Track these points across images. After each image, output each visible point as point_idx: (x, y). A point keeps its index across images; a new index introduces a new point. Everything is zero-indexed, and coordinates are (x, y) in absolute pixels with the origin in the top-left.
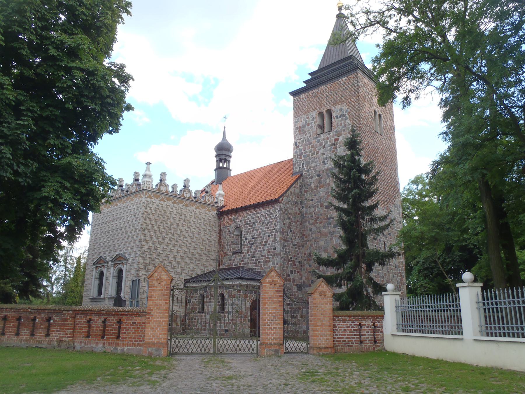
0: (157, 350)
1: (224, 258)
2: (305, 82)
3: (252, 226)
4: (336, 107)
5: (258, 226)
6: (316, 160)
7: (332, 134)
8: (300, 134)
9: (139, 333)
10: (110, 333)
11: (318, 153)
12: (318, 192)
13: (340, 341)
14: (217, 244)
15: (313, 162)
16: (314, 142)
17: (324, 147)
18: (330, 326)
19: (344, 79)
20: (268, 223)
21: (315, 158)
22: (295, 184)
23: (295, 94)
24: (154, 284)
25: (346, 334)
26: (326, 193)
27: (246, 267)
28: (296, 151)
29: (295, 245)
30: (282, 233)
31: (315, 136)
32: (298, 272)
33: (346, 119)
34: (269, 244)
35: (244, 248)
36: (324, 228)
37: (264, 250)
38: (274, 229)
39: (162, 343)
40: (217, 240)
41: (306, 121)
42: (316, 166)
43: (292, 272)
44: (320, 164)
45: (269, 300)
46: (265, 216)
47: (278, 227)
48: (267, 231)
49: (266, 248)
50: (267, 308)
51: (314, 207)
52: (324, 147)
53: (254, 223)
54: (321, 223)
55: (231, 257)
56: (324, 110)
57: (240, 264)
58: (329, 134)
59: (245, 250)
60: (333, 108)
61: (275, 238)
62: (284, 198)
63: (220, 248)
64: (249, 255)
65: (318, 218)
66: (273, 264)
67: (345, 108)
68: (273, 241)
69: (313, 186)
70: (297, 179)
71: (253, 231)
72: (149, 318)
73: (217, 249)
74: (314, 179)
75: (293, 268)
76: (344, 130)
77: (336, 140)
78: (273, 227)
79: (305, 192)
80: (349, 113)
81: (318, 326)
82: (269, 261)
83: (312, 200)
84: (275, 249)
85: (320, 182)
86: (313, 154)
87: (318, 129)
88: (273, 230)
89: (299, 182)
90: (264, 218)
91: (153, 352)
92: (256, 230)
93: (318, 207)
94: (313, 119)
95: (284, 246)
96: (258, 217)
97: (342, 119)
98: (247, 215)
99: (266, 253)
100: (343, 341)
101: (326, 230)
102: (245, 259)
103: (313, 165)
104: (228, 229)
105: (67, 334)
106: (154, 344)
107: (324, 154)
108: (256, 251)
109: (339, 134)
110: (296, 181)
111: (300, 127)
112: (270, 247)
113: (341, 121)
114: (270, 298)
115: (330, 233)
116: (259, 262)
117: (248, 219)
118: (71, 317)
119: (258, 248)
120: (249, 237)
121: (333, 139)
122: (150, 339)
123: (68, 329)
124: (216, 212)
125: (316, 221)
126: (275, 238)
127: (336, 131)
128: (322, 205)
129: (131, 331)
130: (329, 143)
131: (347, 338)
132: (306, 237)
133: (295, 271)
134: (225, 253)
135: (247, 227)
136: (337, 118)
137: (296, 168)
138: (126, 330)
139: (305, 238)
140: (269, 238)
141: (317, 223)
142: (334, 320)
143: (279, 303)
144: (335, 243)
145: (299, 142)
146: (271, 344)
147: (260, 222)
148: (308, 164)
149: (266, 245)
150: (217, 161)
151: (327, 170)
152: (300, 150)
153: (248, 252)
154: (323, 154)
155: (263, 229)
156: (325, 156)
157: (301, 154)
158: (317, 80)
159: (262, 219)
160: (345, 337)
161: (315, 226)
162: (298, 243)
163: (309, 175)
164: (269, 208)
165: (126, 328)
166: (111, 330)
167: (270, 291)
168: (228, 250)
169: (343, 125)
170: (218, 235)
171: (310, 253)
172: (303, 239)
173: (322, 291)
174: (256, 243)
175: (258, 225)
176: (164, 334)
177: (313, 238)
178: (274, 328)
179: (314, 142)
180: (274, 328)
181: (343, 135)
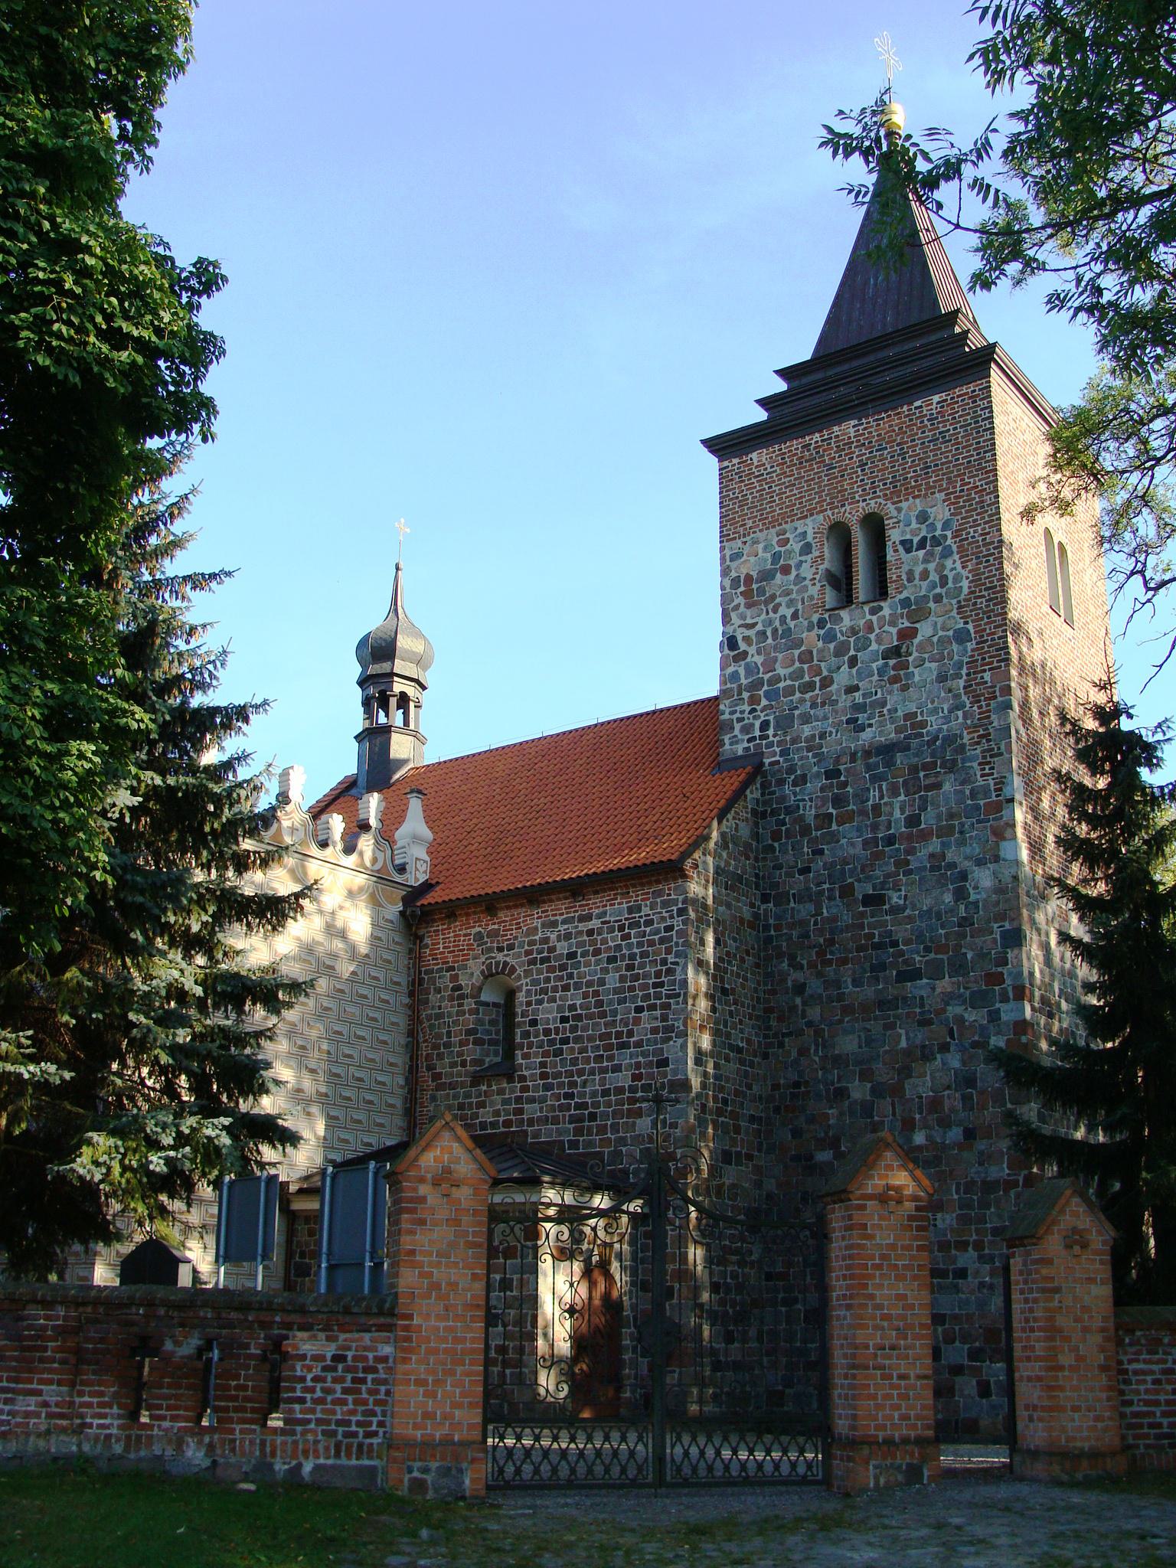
0: (445, 1472)
1: (433, 1098)
2: (763, 403)
3: (563, 968)
4: (904, 505)
5: (589, 969)
7: (886, 612)
8: (748, 606)
9: (365, 1402)
10: (235, 1398)
11: (826, 682)
12: (834, 838)
13: (1141, 1426)
14: (403, 1040)
15: (806, 719)
16: (812, 639)
17: (853, 662)
18: (1104, 1368)
19: (936, 398)
20: (632, 957)
21: (814, 705)
22: (738, 807)
23: (721, 446)
24: (423, 1200)
25: (1162, 1398)
26: (865, 843)
27: (537, 1134)
28: (735, 676)
29: (739, 1050)
31: (815, 618)
32: (749, 1157)
33: (947, 553)
34: (638, 1044)
35: (526, 1056)
36: (856, 982)
37: (617, 1069)
38: (661, 985)
39: (461, 1443)
40: (402, 1021)
41: (776, 557)
42: (822, 736)
45: (879, 1267)
46: (621, 928)
48: (632, 989)
49: (625, 1058)
50: (872, 1297)
51: (816, 899)
52: (853, 662)
53: (572, 955)
54: (844, 961)
55: (468, 1096)
56: (852, 515)
57: (507, 1123)
58: (873, 612)
59: (528, 1063)
60: (891, 508)
61: (664, 1018)
64: (547, 1087)
65: (831, 942)
67: (940, 512)
68: (655, 1030)
69: (810, 814)
71: (566, 988)
72: (408, 1339)
73: (400, 1060)
74: (813, 786)
75: (734, 1142)
76: (938, 599)
77: (907, 635)
78: (658, 974)
79: (777, 835)
81: (1061, 1368)
83: (805, 871)
84: (663, 1063)
85: (839, 801)
86: (809, 687)
87: (828, 589)
88: (655, 985)
89: (753, 794)
90: (614, 939)
91: (429, 1478)
92: (577, 986)
93: (831, 898)
94: (807, 549)
96: (590, 933)
97: (929, 556)
98: (538, 923)
99: (624, 1079)
100: (1151, 1426)
101: (869, 992)
102: (532, 1100)
103: (807, 731)
104: (455, 978)
105: (46, 1404)
106: (427, 1447)
107: (856, 688)
108: (581, 1072)
109: (917, 611)
110: (739, 794)
112: (644, 1054)
113: (926, 561)
114: (883, 1257)
115: (882, 1004)
117: (546, 940)
118: (62, 1332)
119: (587, 1060)
120: (548, 1013)
121: (894, 631)
122: (416, 1426)
123: (50, 1382)
124: (400, 907)
125: (821, 953)
126: (664, 1018)
127: (906, 603)
128: (847, 891)
129: (327, 1391)
130: (874, 646)
131: (1164, 1414)
132: (780, 1019)
133: (738, 1154)
134: (437, 1077)
135: (540, 972)
136: (908, 551)
137: (735, 741)
138: (306, 1390)
139: (774, 1023)
142: (1119, 1343)
143: (915, 1278)
144: (903, 1044)
145: (747, 639)
146: (889, 1442)
147: (597, 952)
148: (784, 723)
149: (624, 1046)
150: (367, 703)
151: (867, 754)
152: (750, 670)
153: (544, 1076)
155: (612, 980)
156: (858, 696)
157: (757, 684)
158: (810, 399)
159: (604, 941)
160: (1158, 1411)
161: (820, 975)
162: (749, 1042)
163: (791, 770)
164: (637, 896)
165: (303, 1379)
166: (238, 1388)
167: (880, 1227)
168: (453, 1065)
169: (934, 577)
170: (407, 1000)
171: (797, 1085)
172: (769, 1028)
173: (1075, 1231)
174: (577, 1040)
175: (588, 964)
176: (471, 1405)
177: (810, 1024)
178: (901, 1377)
179: (812, 639)
180: (901, 1377)
181: (932, 618)
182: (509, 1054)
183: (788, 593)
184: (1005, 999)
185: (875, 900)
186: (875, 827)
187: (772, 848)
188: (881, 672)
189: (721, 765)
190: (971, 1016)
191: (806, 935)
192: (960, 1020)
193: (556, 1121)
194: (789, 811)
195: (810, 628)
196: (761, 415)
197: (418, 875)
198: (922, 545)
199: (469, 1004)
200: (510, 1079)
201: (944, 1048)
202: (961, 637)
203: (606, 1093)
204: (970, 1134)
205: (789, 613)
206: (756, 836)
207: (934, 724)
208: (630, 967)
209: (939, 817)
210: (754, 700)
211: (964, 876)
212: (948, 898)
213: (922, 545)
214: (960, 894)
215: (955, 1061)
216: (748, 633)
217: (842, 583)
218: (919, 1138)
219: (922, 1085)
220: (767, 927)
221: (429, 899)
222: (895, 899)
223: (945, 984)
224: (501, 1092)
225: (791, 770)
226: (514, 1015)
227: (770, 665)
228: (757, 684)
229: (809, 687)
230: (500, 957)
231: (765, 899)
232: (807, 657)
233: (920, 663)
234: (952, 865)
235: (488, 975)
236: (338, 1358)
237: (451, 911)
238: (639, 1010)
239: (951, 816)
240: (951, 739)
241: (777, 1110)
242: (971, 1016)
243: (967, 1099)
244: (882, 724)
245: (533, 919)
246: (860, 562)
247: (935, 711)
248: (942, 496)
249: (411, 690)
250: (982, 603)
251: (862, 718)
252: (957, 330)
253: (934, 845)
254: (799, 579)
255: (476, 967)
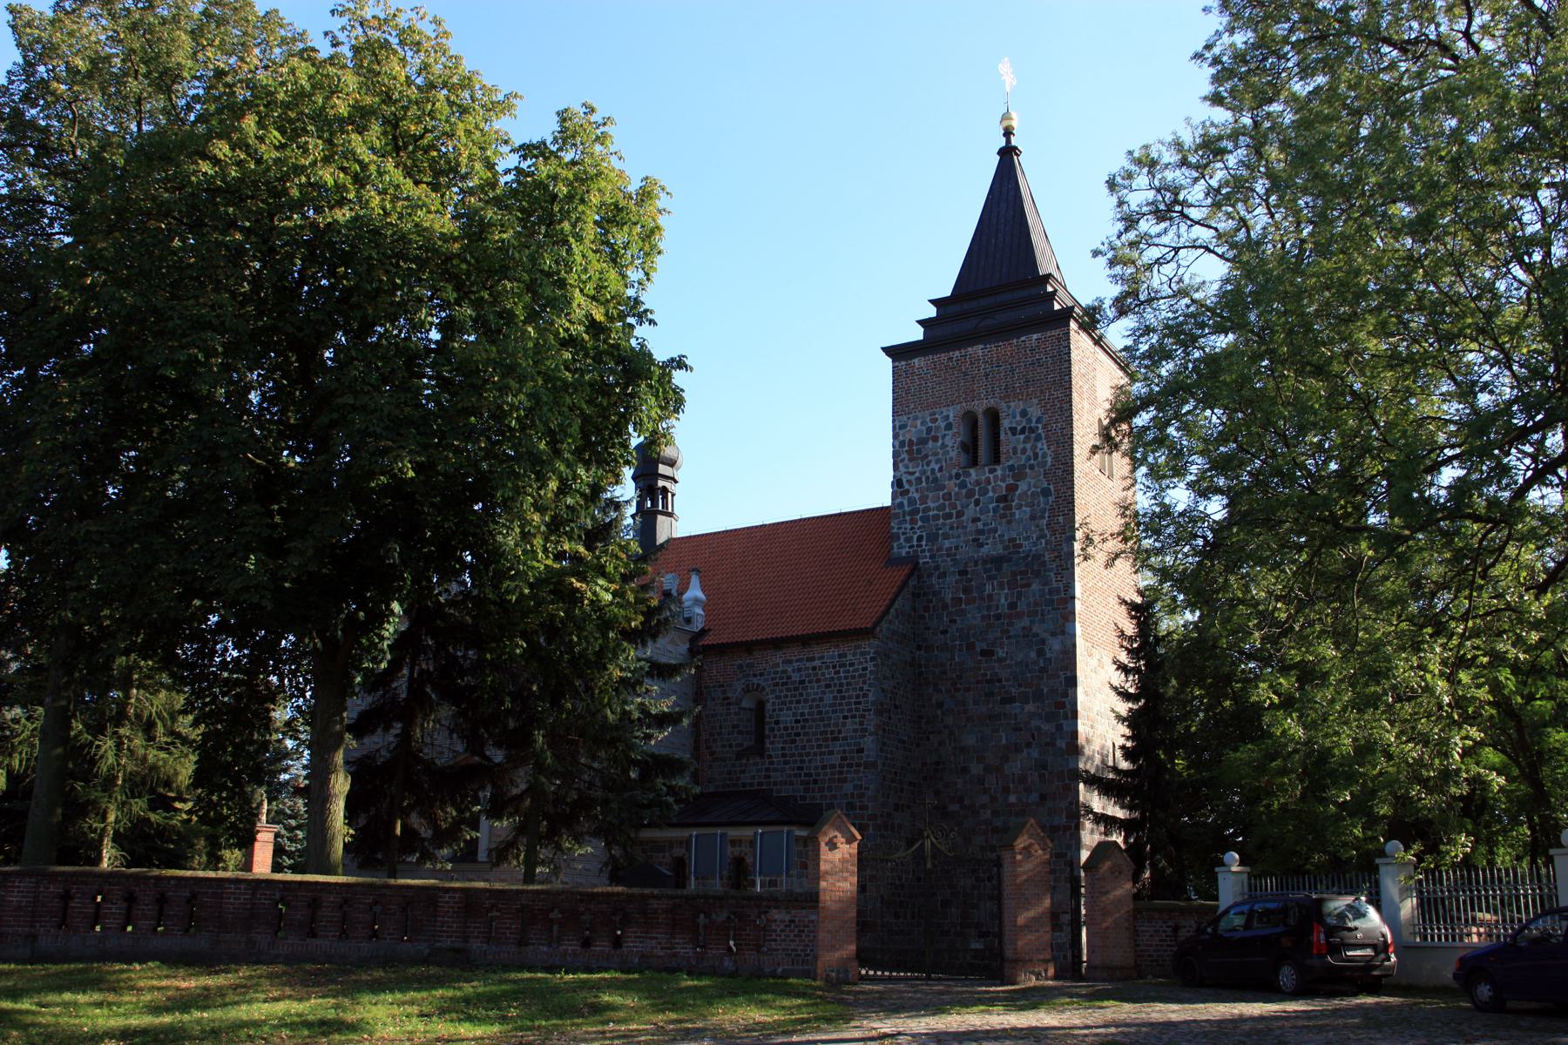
3: (796, 689)
6: (955, 532)
7: (999, 472)
11: (960, 514)
12: (962, 613)
16: (952, 486)
17: (977, 503)
19: (1035, 336)
26: (983, 618)
28: (901, 505)
30: (879, 713)
31: (954, 472)
33: (1038, 438)
34: (845, 739)
36: (975, 703)
37: (831, 753)
41: (929, 430)
42: (957, 548)
43: (897, 807)
44: (966, 542)
47: (871, 698)
53: (802, 682)
54: (968, 690)
56: (979, 407)
57: (760, 784)
58: (991, 471)
59: (774, 746)
60: (1003, 405)
61: (861, 723)
62: (884, 625)
63: (697, 741)
64: (786, 763)
65: (960, 677)
66: (855, 787)
67: (1035, 411)
68: (855, 731)
70: (909, 576)
71: (798, 702)
74: (951, 579)
76: (1032, 467)
77: (1012, 488)
78: (858, 696)
79: (926, 609)
80: (1045, 427)
82: (845, 781)
83: (945, 632)
84: (861, 751)
85: (966, 590)
86: (949, 516)
92: (806, 701)
94: (949, 427)
95: (884, 744)
96: (814, 668)
98: (780, 661)
99: (835, 759)
102: (776, 770)
103: (947, 544)
104: (724, 692)
107: (978, 520)
108: (808, 754)
109: (1018, 473)
110: (905, 584)
111: (911, 442)
116: (815, 782)
117: (784, 672)
120: (787, 717)
125: (954, 684)
126: (861, 723)
127: (1011, 468)
128: (971, 647)
134: (712, 754)
137: (901, 547)
140: (844, 724)
141: (957, 690)
145: (909, 482)
147: (818, 681)
148: (932, 538)
149: (836, 739)
151: (985, 562)
152: (912, 502)
153: (784, 755)
154: (976, 520)
157: (915, 512)
163: (937, 568)
169: (1029, 453)
171: (937, 763)
174: (806, 734)
182: (760, 737)
183: (936, 454)
184: (1066, 718)
185: (987, 653)
186: (989, 608)
187: (923, 617)
188: (995, 510)
189: (893, 561)
190: (1046, 727)
191: (945, 673)
192: (1039, 729)
193: (791, 783)
194: (934, 594)
195: (950, 478)
196: (918, 334)
197: (698, 625)
198: (1023, 431)
199: (734, 709)
200: (762, 756)
201: (1029, 745)
202: (1046, 492)
203: (824, 767)
204: (1043, 797)
205: (937, 467)
206: (914, 609)
207: (1026, 546)
208: (840, 691)
209: (1029, 605)
210: (913, 521)
211: (1043, 642)
212: (1033, 655)
213: (1023, 431)
214: (1041, 653)
215: (1035, 755)
216: (912, 478)
217: (970, 449)
218: (1012, 799)
219: (1015, 766)
220: (920, 666)
221: (708, 640)
222: (1001, 653)
223: (1030, 707)
224: (756, 764)
225: (937, 568)
226: (764, 717)
227: (924, 499)
228: (915, 512)
229: (949, 516)
230: (755, 680)
231: (919, 648)
232: (948, 497)
233: (1019, 507)
234: (1037, 635)
235: (747, 690)
236: (792, 921)
237: (722, 649)
238: (845, 717)
239: (1036, 604)
240: (1037, 557)
241: (925, 778)
242: (1046, 727)
243: (1041, 776)
244: (995, 544)
245: (778, 658)
246: (982, 439)
247: (1027, 538)
248: (1035, 401)
249: (667, 484)
250: (1059, 473)
251: (982, 538)
252: (1050, 289)
253: (1026, 622)
254: (944, 446)
255: (739, 686)
